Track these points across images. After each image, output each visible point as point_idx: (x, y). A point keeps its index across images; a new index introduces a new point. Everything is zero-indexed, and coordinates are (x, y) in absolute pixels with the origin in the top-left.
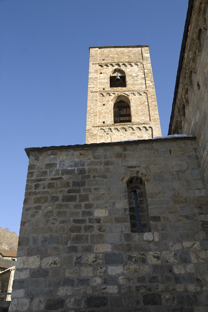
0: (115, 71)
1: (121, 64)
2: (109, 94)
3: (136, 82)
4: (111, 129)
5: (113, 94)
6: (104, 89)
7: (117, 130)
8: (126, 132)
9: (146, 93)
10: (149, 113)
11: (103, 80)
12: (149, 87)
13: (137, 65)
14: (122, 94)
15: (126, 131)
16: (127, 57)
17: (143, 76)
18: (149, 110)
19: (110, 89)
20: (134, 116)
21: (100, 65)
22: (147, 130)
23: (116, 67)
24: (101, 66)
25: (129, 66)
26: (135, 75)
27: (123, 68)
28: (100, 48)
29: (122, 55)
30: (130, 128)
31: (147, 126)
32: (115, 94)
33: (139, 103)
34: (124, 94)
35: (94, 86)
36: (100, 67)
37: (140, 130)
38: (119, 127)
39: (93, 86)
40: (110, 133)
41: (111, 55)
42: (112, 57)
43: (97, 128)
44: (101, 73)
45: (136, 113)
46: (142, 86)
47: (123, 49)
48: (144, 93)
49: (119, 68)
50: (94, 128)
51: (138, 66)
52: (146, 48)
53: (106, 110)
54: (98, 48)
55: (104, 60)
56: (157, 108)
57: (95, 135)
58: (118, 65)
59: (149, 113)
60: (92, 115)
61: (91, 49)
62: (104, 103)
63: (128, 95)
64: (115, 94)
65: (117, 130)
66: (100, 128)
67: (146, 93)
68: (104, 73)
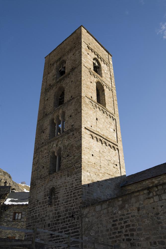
0: (95, 59)
1: (99, 57)
2: (94, 76)
4: (96, 106)
5: (96, 77)
7: (100, 109)
8: (103, 114)
9: (112, 91)
10: (114, 108)
13: (107, 65)
14: (100, 81)
15: (103, 113)
17: (110, 77)
18: (114, 105)
19: (93, 71)
21: (87, 46)
22: (113, 120)
23: (96, 57)
24: (89, 48)
25: (103, 62)
27: (99, 60)
28: (88, 32)
29: (99, 49)
30: (105, 112)
31: (114, 117)
32: (97, 78)
34: (101, 83)
35: (85, 61)
36: (88, 48)
37: (110, 117)
38: (101, 108)
40: (95, 108)
43: (89, 100)
44: (88, 54)
47: (99, 46)
48: (111, 90)
49: (98, 58)
50: (86, 98)
51: (107, 66)
52: (110, 56)
53: (92, 88)
54: (86, 31)
56: (117, 106)
57: (88, 105)
58: (98, 57)
59: (114, 108)
61: (82, 27)
63: (103, 85)
64: (97, 78)
65: (100, 109)
66: (90, 101)
67: (112, 91)
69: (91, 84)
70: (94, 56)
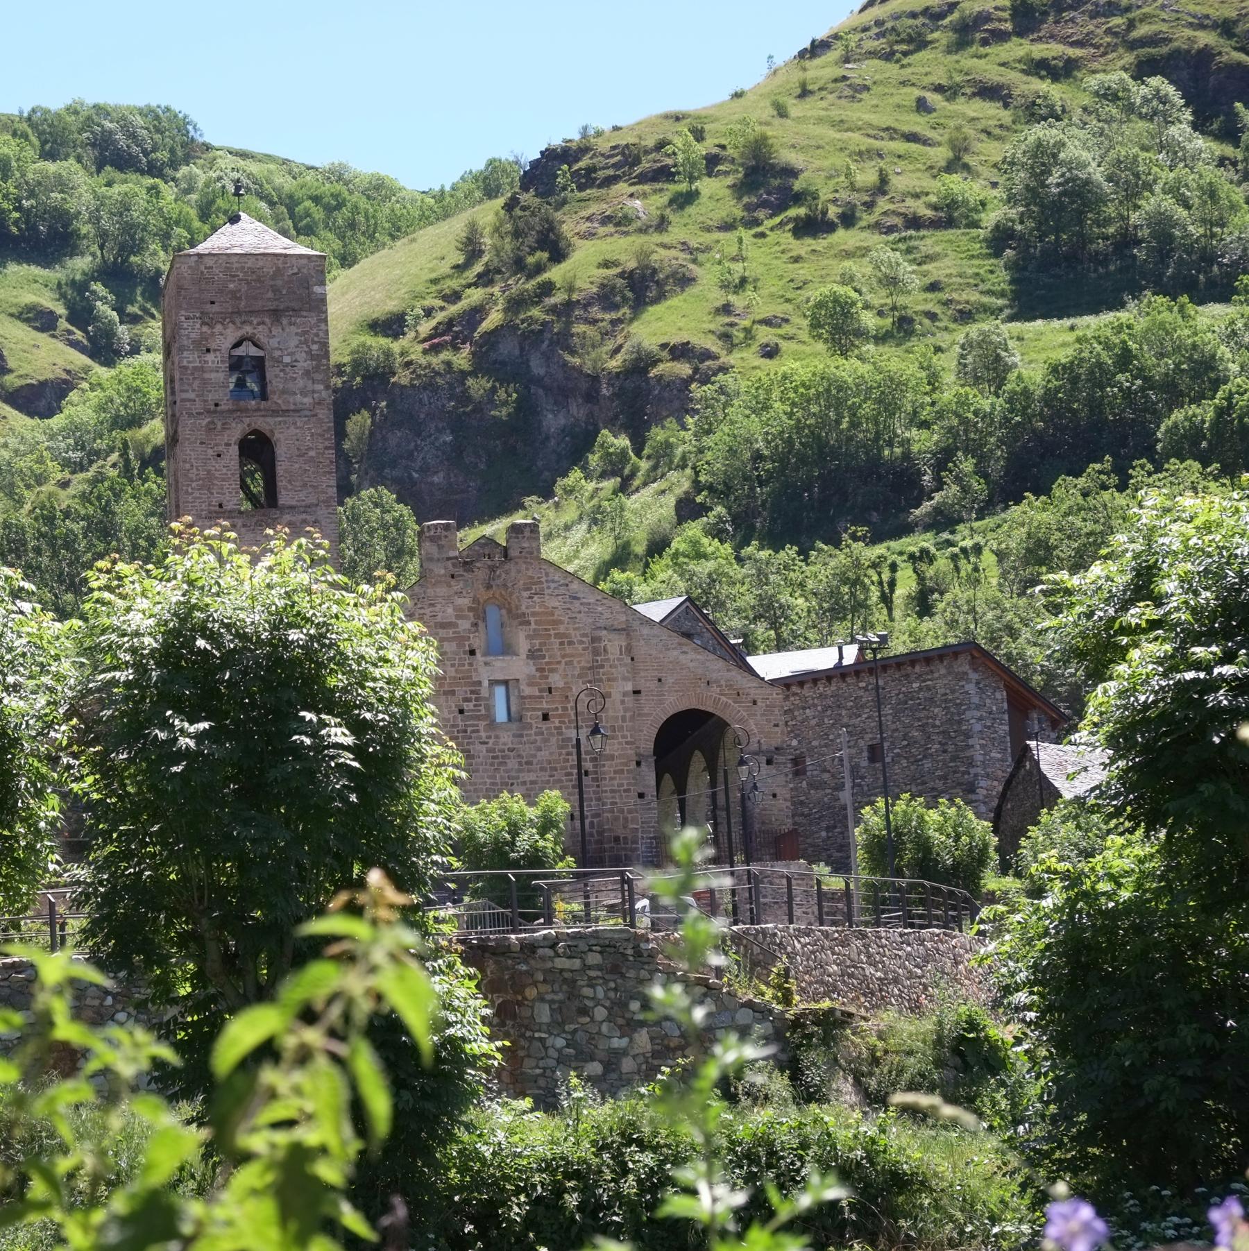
3: (290, 385)
6: (217, 405)
11: (213, 375)
12: (319, 403)
16: (270, 295)
20: (286, 489)
26: (287, 359)
27: (261, 333)
33: (297, 453)
39: (192, 395)
41: (231, 286)
42: (233, 293)
44: (208, 351)
45: (290, 481)
46: (306, 400)
55: (213, 303)
60: (194, 485)
62: (220, 448)
68: (215, 350)
69: (222, 462)
70: (232, 335)
